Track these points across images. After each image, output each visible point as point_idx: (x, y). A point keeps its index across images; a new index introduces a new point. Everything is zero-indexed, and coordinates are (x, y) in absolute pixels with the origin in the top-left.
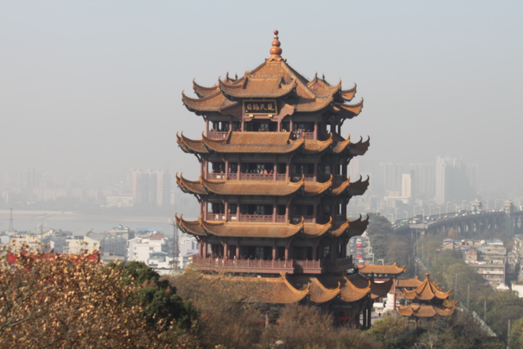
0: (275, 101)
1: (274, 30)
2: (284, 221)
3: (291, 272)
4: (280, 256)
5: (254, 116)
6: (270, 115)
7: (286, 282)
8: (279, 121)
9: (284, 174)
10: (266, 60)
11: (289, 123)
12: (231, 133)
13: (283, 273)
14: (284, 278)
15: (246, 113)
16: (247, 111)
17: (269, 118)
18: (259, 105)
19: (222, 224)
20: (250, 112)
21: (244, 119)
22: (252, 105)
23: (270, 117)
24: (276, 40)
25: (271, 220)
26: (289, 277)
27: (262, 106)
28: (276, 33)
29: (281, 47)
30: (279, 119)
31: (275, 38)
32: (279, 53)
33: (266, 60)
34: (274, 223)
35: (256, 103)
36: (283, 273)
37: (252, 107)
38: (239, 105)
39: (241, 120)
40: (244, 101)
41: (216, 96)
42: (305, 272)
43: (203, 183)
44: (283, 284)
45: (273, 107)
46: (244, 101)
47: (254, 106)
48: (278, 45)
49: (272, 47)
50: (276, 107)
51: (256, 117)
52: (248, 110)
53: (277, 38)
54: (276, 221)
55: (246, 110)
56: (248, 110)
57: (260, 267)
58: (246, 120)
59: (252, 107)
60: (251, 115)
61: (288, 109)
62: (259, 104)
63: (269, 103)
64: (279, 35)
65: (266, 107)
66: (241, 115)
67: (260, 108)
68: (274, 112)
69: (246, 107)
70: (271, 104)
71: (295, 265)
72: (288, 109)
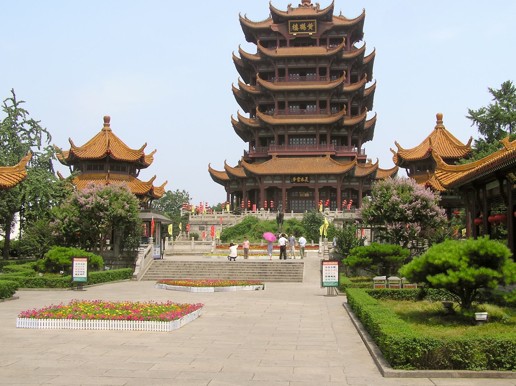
0: (315, 20)
6: (311, 34)
17: (309, 36)
40: (289, 21)
45: (314, 28)
46: (289, 21)
58: (291, 39)
60: (295, 34)
70: (312, 24)
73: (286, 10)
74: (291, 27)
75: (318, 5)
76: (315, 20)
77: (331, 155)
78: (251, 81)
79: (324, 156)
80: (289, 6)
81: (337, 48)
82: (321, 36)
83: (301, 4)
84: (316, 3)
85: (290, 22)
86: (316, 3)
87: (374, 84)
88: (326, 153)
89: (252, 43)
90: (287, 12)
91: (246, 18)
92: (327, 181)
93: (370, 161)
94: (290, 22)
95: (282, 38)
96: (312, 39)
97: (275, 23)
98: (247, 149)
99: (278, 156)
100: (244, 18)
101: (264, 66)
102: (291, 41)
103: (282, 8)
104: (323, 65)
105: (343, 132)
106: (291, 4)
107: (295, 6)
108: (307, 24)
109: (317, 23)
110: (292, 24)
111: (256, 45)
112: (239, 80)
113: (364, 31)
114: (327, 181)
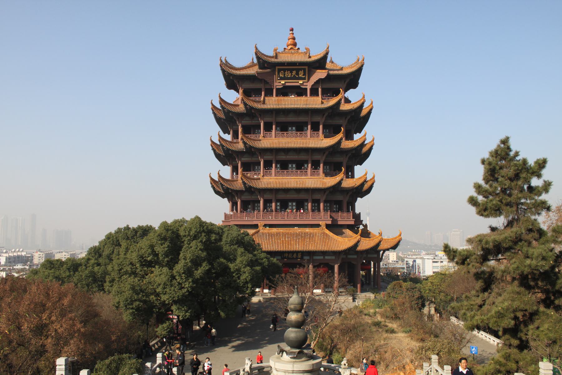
0: (306, 67)
1: (290, 27)
2: (318, 175)
3: (330, 222)
4: (316, 209)
5: (285, 82)
6: (301, 82)
7: (327, 232)
8: (309, 88)
10: (285, 49)
11: (318, 89)
12: (264, 98)
13: (323, 223)
14: (325, 227)
15: (278, 80)
16: (279, 78)
17: (299, 85)
18: (291, 72)
19: (259, 179)
20: (282, 79)
21: (276, 86)
22: (285, 72)
23: (300, 84)
24: (292, 35)
25: (306, 174)
26: (328, 226)
27: (294, 73)
28: (292, 30)
29: (296, 41)
30: (309, 86)
31: (290, 34)
32: (295, 44)
33: (285, 49)
34: (310, 177)
35: (288, 70)
36: (323, 223)
37: (284, 75)
38: (273, 72)
39: (274, 86)
40: (277, 68)
41: (248, 68)
42: (339, 223)
43: (243, 137)
44: (324, 233)
45: (304, 74)
46: (277, 68)
47: (286, 73)
48: (294, 39)
49: (288, 41)
50: (307, 75)
51: (287, 84)
52: (280, 77)
53: (293, 34)
54: (311, 176)
56: (280, 77)
57: (298, 219)
58: (277, 87)
59: (284, 75)
60: (283, 82)
61: (320, 74)
62: (291, 71)
63: (301, 69)
64: (293, 32)
65: (297, 74)
66: (274, 82)
67: (292, 75)
68: (304, 79)
69: (279, 74)
70: (302, 71)
71: (331, 217)
72: (320, 74)
73: (271, 53)
74: (279, 74)
76: (306, 67)
78: (231, 132)
79: (318, 226)
80: (275, 50)
81: (333, 101)
82: (313, 86)
83: (286, 47)
85: (278, 69)
87: (372, 141)
88: (320, 223)
89: (233, 91)
91: (226, 61)
92: (324, 257)
93: (366, 226)
94: (278, 69)
95: (268, 87)
96: (302, 88)
97: (260, 68)
98: (228, 212)
99: (265, 226)
100: (224, 62)
102: (277, 89)
103: (268, 51)
104: (316, 119)
105: (339, 197)
107: (280, 50)
110: (279, 71)
111: (237, 92)
112: (219, 135)
113: (359, 81)
114: (324, 257)
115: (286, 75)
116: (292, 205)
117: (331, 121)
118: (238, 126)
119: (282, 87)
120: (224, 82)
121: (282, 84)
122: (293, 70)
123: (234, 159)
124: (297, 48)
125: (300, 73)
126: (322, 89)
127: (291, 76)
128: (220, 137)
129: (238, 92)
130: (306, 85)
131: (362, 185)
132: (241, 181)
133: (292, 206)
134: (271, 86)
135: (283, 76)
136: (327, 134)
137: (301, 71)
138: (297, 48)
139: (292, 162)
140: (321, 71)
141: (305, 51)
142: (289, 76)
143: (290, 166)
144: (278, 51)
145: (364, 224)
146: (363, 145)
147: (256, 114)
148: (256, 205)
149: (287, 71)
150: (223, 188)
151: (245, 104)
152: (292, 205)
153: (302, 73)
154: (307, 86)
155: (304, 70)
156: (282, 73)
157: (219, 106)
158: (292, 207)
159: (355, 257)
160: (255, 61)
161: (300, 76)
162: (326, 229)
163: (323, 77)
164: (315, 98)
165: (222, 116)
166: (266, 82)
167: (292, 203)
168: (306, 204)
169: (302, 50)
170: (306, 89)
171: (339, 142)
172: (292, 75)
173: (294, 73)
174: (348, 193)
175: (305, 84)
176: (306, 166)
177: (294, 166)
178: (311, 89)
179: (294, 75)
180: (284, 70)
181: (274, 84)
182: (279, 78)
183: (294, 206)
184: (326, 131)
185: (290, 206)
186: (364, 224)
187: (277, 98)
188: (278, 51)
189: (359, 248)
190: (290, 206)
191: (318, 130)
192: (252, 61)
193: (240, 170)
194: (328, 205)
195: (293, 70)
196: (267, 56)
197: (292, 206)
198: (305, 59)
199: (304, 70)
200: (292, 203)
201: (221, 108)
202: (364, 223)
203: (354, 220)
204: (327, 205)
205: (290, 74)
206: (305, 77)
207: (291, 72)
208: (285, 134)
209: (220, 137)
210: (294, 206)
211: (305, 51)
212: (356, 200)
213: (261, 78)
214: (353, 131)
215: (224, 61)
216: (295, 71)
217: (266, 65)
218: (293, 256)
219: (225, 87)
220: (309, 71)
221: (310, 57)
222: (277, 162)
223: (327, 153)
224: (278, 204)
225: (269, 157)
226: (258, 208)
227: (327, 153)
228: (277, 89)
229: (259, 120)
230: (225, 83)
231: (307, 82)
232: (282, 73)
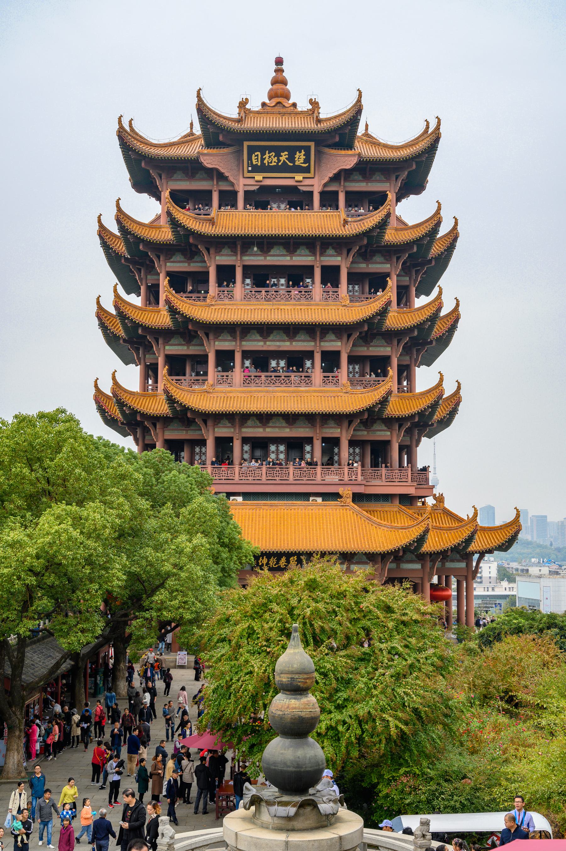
0: (312, 144)
9: (335, 289)
10: (264, 104)
14: (350, 500)
15: (249, 172)
16: (250, 169)
18: (278, 155)
20: (256, 169)
22: (263, 154)
23: (297, 181)
26: (358, 498)
27: (284, 156)
33: (264, 104)
35: (271, 149)
39: (238, 185)
40: (246, 144)
45: (307, 160)
46: (246, 144)
47: (267, 155)
52: (252, 165)
55: (248, 166)
59: (263, 160)
60: (259, 177)
62: (278, 151)
63: (299, 149)
64: (284, 67)
65: (291, 158)
67: (279, 161)
68: (307, 170)
69: (250, 158)
70: (303, 152)
74: (250, 158)
75: (315, 104)
76: (312, 144)
77: (354, 494)
79: (336, 496)
80: (243, 104)
82: (325, 185)
83: (267, 101)
84: (311, 100)
85: (248, 146)
86: (311, 100)
90: (239, 121)
93: (440, 499)
94: (248, 146)
95: (225, 187)
101: (178, 257)
104: (332, 259)
106: (247, 99)
107: (254, 105)
108: (292, 151)
109: (315, 155)
110: (251, 150)
111: (157, 200)
112: (115, 290)
113: (428, 178)
115: (266, 162)
116: (277, 450)
117: (364, 265)
118: (158, 274)
119: (258, 187)
120: (126, 175)
121: (257, 181)
122: (284, 149)
123: (148, 348)
124: (291, 101)
125: (297, 156)
126: (348, 194)
127: (278, 163)
128: (117, 296)
129: (159, 198)
130: (310, 184)
131: (434, 406)
132: (164, 397)
133: (277, 452)
134: (232, 184)
135: (259, 164)
136: (357, 294)
137: (300, 152)
138: (291, 101)
139: (278, 355)
140: (343, 152)
141: (310, 107)
142: (273, 164)
143: (273, 363)
144: (248, 106)
145: (437, 495)
146: (434, 318)
147: (199, 247)
148: (197, 450)
149: (269, 153)
150: (123, 412)
151: (174, 223)
152: (277, 450)
153: (303, 157)
154: (313, 186)
155: (307, 150)
156: (257, 155)
157: (114, 229)
158: (277, 455)
159: (418, 566)
160: (198, 130)
161: (297, 163)
162: (352, 504)
163: (348, 167)
164: (330, 212)
165: (121, 248)
166: (221, 177)
167: (277, 447)
168: (308, 448)
169: (304, 106)
170: (311, 193)
171: (383, 312)
172: (279, 161)
173: (284, 156)
174: (400, 426)
175: (307, 182)
176: (308, 364)
177: (282, 363)
178: (323, 194)
179: (284, 161)
180: (263, 150)
181: (239, 181)
182: (250, 169)
183: (282, 452)
184: (353, 287)
185: (273, 452)
186: (437, 495)
187: (246, 213)
188: (248, 106)
189: (427, 547)
190: (273, 452)
191: (336, 284)
192: (189, 130)
193: (163, 371)
194: (357, 450)
195: (284, 149)
196: (225, 118)
197: (277, 452)
198: (308, 125)
199: (307, 150)
200: (277, 447)
201: (119, 234)
202: (437, 491)
203: (415, 484)
204: (354, 452)
205: (275, 159)
206: (309, 165)
207: (278, 155)
208: (263, 293)
209: (117, 296)
210: (282, 452)
211: (310, 107)
212: (418, 442)
213: (209, 166)
214: (414, 289)
215: (127, 128)
216: (286, 153)
217: (221, 138)
218: (278, 563)
219: (129, 184)
220: (319, 153)
221: (319, 121)
222: (246, 354)
223: (356, 335)
224: (247, 448)
225: (227, 343)
226: (200, 456)
227: (356, 335)
228: (246, 192)
229: (205, 262)
230: (128, 176)
231: (313, 178)
232: (257, 155)
